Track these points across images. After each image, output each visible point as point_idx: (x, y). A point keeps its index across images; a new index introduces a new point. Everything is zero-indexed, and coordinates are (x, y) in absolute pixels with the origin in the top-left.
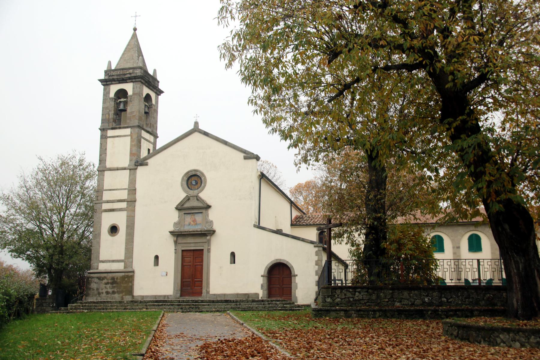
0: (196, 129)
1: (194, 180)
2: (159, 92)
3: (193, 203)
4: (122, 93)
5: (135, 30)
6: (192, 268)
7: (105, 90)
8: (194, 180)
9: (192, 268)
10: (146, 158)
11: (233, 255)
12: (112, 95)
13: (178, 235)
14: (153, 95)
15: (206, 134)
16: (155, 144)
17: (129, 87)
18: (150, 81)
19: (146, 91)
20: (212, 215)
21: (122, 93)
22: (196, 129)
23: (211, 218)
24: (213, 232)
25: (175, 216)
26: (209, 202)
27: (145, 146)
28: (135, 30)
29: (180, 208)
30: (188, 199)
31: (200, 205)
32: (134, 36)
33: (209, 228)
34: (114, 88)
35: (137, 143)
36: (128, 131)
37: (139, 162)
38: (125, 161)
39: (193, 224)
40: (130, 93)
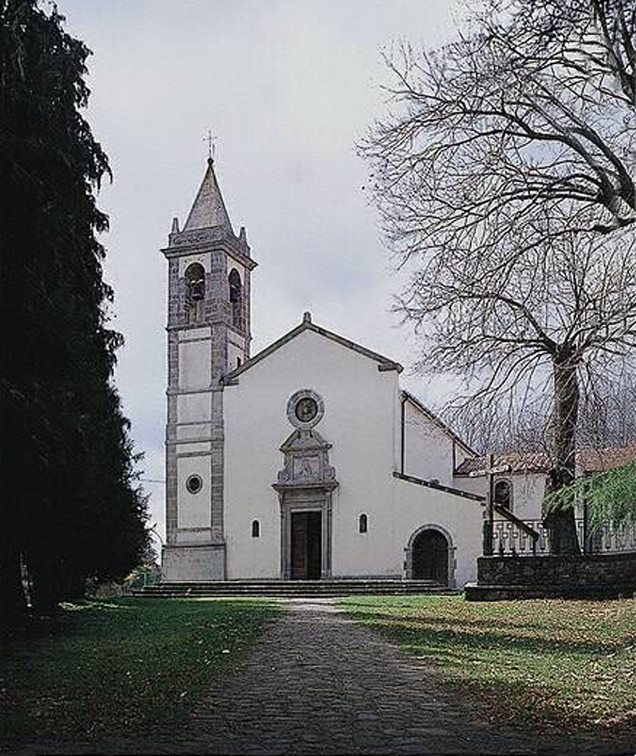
0: (307, 324)
1: (306, 407)
2: (251, 266)
3: (306, 442)
4: (197, 270)
5: (211, 161)
6: (306, 540)
7: (171, 265)
8: (306, 407)
9: (306, 540)
10: (235, 374)
11: (363, 519)
12: (181, 274)
13: (285, 491)
14: (241, 271)
15: (322, 332)
16: (247, 350)
17: (206, 261)
18: (237, 247)
19: (232, 265)
20: (334, 459)
21: (197, 270)
22: (307, 324)
23: (331, 464)
24: (335, 485)
25: (279, 462)
26: (330, 439)
27: (235, 354)
28: (211, 161)
29: (287, 449)
30: (298, 435)
31: (315, 443)
32: (210, 169)
33: (328, 479)
34: (184, 263)
35: (220, 352)
36: (206, 332)
37: (226, 380)
38: (206, 379)
39: (306, 472)
40: (208, 269)
